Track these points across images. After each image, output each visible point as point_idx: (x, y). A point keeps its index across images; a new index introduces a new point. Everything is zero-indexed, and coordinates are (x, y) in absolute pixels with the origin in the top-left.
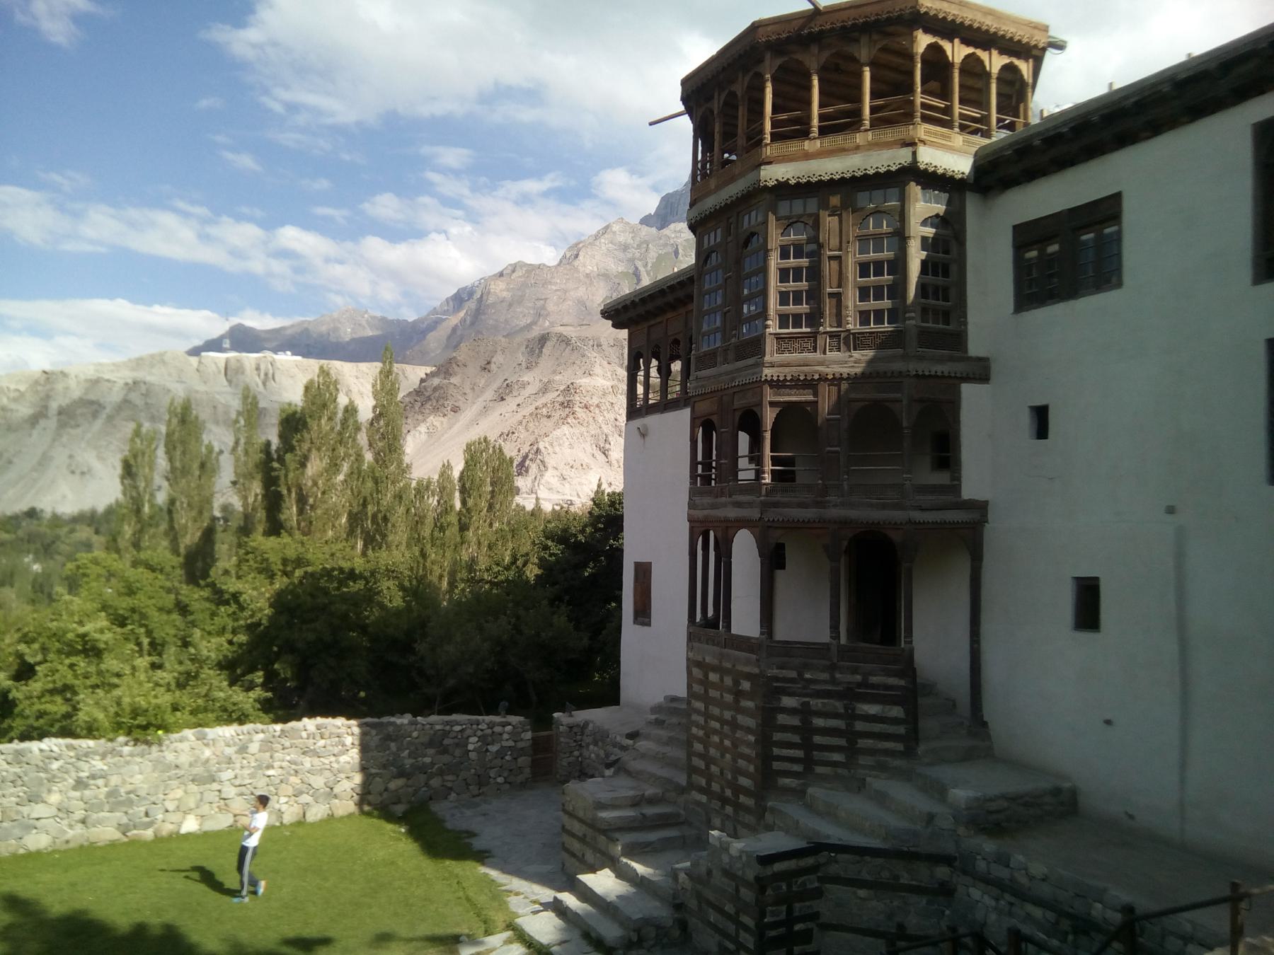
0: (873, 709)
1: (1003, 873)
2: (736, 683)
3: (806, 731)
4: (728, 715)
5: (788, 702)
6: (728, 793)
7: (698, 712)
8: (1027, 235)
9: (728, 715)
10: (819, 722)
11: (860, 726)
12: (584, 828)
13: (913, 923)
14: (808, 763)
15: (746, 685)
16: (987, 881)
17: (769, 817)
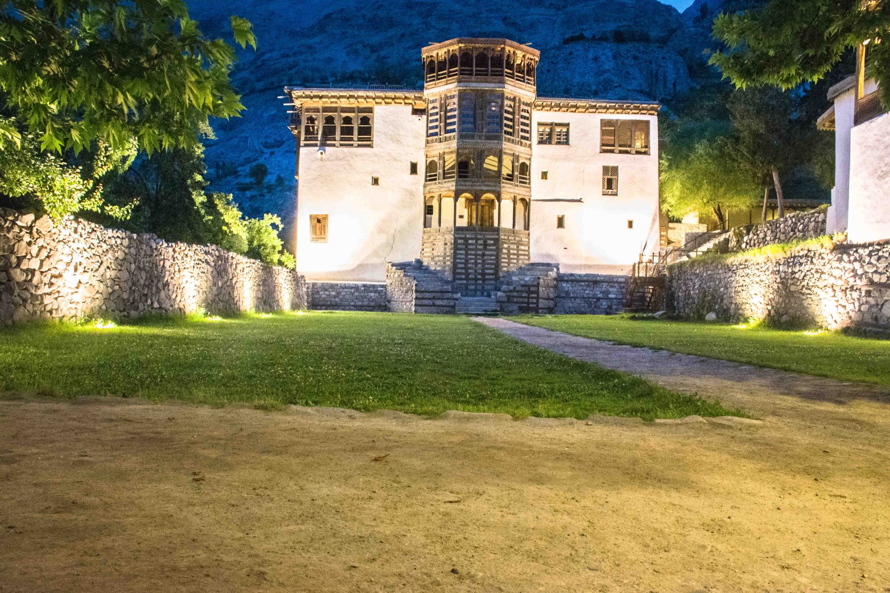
0: (522, 247)
1: (573, 278)
2: (485, 242)
3: (509, 254)
4: (480, 252)
5: (506, 246)
6: (479, 277)
7: (461, 254)
8: (540, 124)
9: (480, 252)
10: (512, 251)
11: (520, 252)
12: (434, 294)
13: (551, 296)
14: (509, 263)
15: (492, 242)
16: (567, 281)
17: (502, 279)
